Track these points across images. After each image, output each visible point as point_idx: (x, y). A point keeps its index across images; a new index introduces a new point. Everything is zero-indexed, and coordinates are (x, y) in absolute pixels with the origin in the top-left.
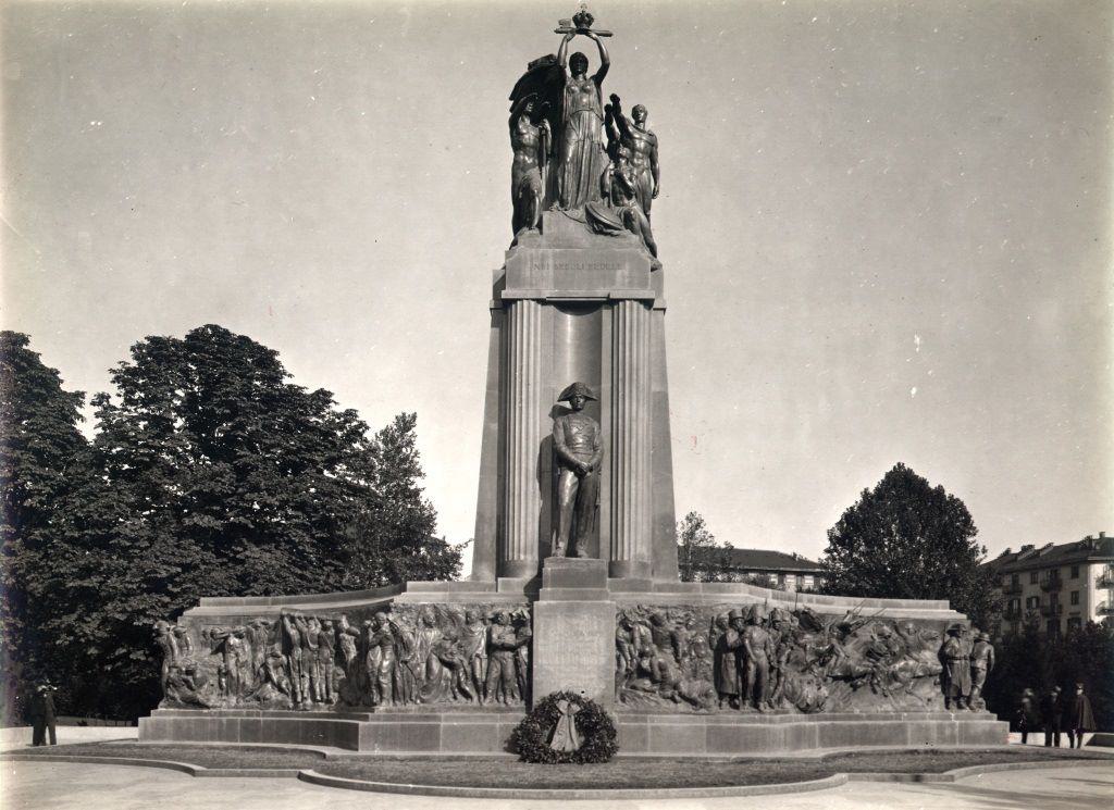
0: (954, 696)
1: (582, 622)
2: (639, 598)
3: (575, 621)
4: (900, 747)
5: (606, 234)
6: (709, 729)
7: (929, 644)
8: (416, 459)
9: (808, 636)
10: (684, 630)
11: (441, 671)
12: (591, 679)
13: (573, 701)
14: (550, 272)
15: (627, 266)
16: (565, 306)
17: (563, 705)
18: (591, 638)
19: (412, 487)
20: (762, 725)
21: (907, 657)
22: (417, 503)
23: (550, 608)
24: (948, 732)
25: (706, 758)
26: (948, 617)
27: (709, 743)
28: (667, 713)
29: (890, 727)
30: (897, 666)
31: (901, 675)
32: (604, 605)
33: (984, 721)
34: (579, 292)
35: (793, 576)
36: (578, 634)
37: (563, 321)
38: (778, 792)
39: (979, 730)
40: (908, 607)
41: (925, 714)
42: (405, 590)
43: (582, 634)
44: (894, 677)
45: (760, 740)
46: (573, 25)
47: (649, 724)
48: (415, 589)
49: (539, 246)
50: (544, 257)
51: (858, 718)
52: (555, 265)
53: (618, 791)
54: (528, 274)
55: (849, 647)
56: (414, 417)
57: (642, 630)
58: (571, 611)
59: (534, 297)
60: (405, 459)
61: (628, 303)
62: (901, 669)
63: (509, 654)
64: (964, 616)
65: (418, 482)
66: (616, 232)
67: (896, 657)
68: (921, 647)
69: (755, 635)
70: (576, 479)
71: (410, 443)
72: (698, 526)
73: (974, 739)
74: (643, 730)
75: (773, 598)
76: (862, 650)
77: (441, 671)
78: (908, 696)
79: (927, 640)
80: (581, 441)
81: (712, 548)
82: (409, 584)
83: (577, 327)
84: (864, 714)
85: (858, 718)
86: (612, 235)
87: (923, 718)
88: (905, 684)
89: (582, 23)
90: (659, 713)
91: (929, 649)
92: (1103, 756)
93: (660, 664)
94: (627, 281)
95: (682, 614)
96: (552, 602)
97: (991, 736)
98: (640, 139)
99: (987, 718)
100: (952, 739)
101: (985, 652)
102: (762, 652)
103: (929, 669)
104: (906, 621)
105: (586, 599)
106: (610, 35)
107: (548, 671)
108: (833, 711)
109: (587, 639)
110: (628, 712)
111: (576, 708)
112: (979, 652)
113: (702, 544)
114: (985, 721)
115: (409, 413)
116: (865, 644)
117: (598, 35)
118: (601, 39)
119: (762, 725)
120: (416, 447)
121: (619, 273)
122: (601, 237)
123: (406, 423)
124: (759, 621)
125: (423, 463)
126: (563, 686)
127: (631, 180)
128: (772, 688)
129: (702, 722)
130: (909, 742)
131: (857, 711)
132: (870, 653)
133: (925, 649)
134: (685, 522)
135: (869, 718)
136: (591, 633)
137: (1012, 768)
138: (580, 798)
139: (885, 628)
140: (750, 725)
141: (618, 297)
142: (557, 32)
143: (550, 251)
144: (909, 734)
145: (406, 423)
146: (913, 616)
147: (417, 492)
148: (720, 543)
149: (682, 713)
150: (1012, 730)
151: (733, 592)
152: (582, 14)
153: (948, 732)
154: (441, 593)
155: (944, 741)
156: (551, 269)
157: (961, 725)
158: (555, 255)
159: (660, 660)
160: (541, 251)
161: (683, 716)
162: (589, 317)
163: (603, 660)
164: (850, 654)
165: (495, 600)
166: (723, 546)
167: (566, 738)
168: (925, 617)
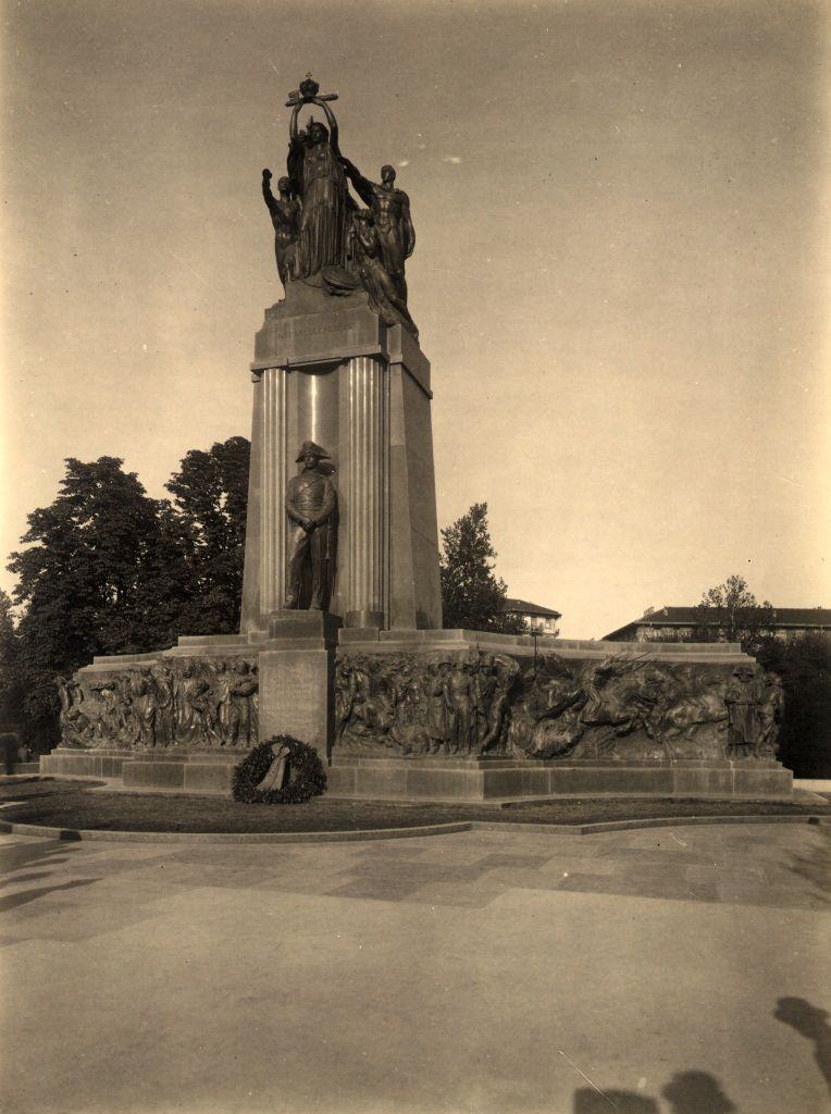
0: (739, 744)
1: (299, 671)
2: (362, 648)
3: (292, 671)
4: (667, 796)
5: (340, 295)
6: (410, 772)
7: (709, 689)
8: (488, 541)
9: (554, 682)
10: (399, 677)
11: (191, 718)
12: (307, 724)
13: (286, 745)
14: (291, 340)
15: (358, 323)
16: (308, 370)
17: (275, 748)
18: (305, 686)
19: (485, 565)
20: (463, 771)
21: (685, 702)
22: (486, 578)
23: (272, 657)
24: (722, 781)
25: (393, 802)
26: (734, 660)
27: (409, 788)
28: (378, 757)
29: (655, 773)
30: (675, 712)
31: (679, 721)
32: (318, 654)
33: (766, 768)
34: (316, 356)
35: (784, 631)
36: (296, 681)
37: (310, 381)
38: (313, 840)
39: (760, 778)
40: (693, 650)
41: (706, 760)
42: (177, 645)
43: (298, 681)
44: (669, 723)
45: (456, 785)
46: (301, 96)
47: (355, 769)
48: (186, 643)
49: (283, 316)
50: (286, 325)
51: (615, 764)
52: (295, 333)
53: (128, 833)
54: (273, 344)
55: (609, 692)
56: (485, 506)
57: (359, 679)
58: (291, 660)
59: (279, 364)
60: (480, 542)
61: (357, 359)
62: (678, 715)
63: (243, 701)
64: (754, 659)
65: (489, 561)
66: (347, 293)
67: (672, 703)
68: (698, 692)
69: (454, 681)
70: (305, 534)
71: (482, 529)
72: (741, 588)
73: (752, 789)
74: (351, 773)
75: (518, 644)
76: (624, 695)
77: (191, 718)
78: (688, 743)
79: (709, 685)
80: (308, 498)
81: (753, 608)
82: (180, 638)
83: (322, 391)
84: (623, 761)
85: (615, 764)
86: (346, 296)
87: (698, 765)
88: (683, 730)
89: (309, 92)
90: (372, 757)
91: (711, 694)
92: (476, 812)
93: (368, 709)
94: (357, 339)
95: (396, 661)
96: (275, 652)
97: (772, 785)
98: (385, 199)
99: (771, 766)
100: (728, 788)
101: (772, 696)
102: (463, 698)
103: (606, 714)
104: (687, 664)
105: (302, 648)
106: (334, 98)
107: (271, 716)
108: (585, 756)
109: (303, 686)
110: (345, 755)
111: (287, 750)
112: (768, 696)
113: (744, 605)
114: (768, 770)
115: (480, 502)
116: (627, 689)
117: (324, 100)
118: (329, 103)
119: (641, 769)
120: (487, 532)
121: (350, 332)
122: (336, 298)
123: (479, 512)
124: (460, 666)
125: (493, 543)
126: (283, 729)
127: (368, 240)
128: (482, 734)
129: (407, 766)
130: (675, 789)
131: (617, 757)
132: (632, 697)
133: (706, 693)
134: (726, 585)
135: (630, 764)
136: (306, 681)
137: (719, 822)
138: (96, 839)
139: (657, 672)
140: (452, 771)
141: (350, 355)
142: (288, 105)
143: (292, 319)
144: (675, 783)
145: (479, 512)
146: (689, 660)
147: (487, 570)
148: (760, 603)
149: (391, 757)
150: (795, 777)
151: (450, 638)
152: (309, 82)
153: (722, 781)
154: (202, 647)
155: (716, 789)
156: (292, 335)
157: (738, 774)
158: (295, 322)
159: (371, 706)
160: (284, 320)
161: (392, 760)
162: (330, 377)
163: (316, 707)
164: (610, 700)
165: (241, 652)
166: (762, 606)
167: (274, 779)
168: (709, 661)
